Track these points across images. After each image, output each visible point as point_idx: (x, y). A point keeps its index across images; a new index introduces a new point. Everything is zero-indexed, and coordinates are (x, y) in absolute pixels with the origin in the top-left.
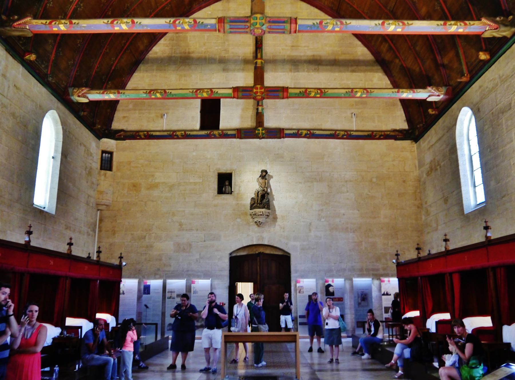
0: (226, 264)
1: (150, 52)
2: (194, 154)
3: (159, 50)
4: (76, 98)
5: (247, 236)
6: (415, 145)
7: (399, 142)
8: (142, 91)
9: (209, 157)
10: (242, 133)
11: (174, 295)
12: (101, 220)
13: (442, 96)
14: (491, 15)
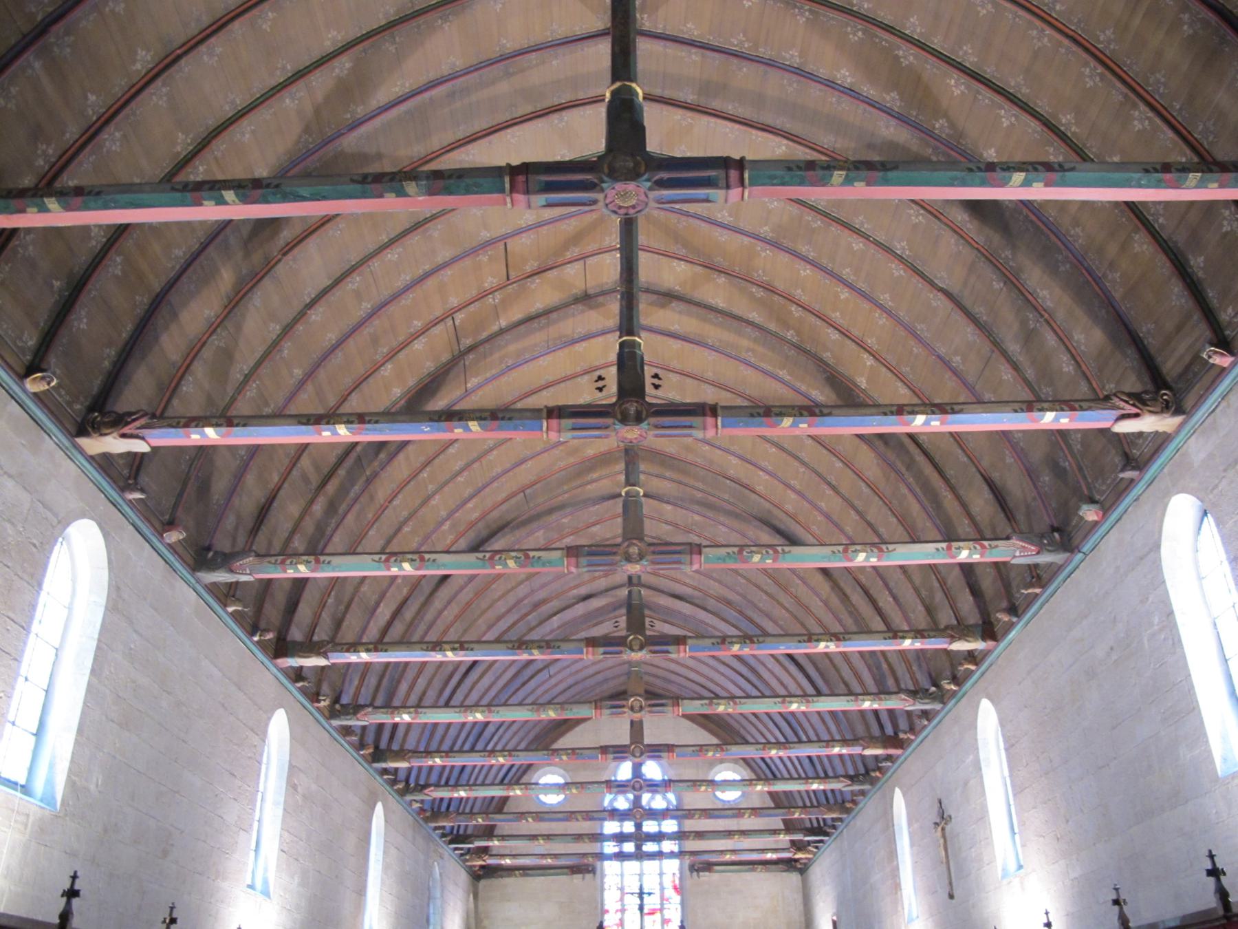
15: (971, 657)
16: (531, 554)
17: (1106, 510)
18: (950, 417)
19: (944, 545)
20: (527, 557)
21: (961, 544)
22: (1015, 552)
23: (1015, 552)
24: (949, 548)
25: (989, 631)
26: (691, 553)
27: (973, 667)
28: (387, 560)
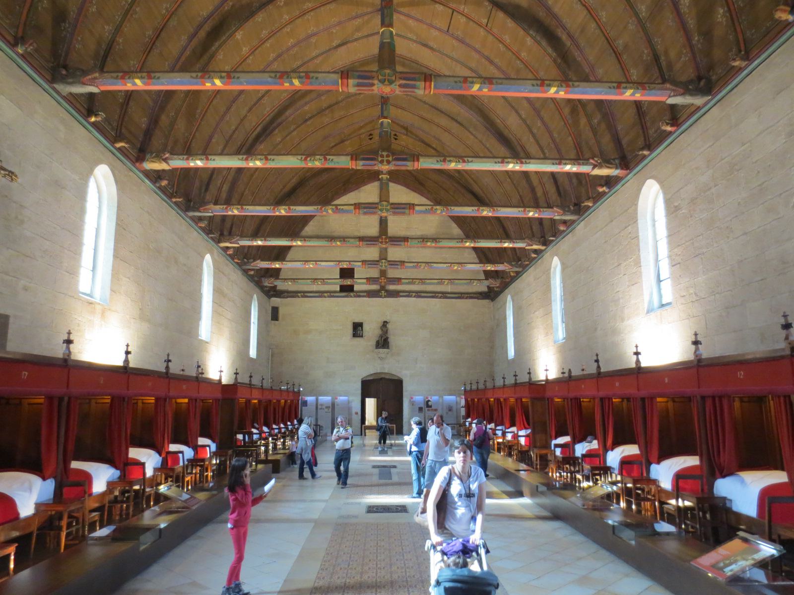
0: (359, 386)
1: (303, 231)
2: (336, 308)
3: (309, 229)
4: (266, 284)
5: (372, 365)
6: (492, 303)
7: (480, 301)
8: (309, 280)
9: (347, 311)
10: (371, 294)
11: (324, 407)
12: (272, 356)
13: (498, 285)
14: (509, 263)
15: (535, 251)
16: (339, 207)
17: (595, 203)
18: (524, 165)
19: (522, 209)
20: (337, 208)
21: (530, 209)
22: (555, 214)
23: (555, 214)
24: (524, 211)
25: (546, 243)
26: (410, 209)
27: (535, 256)
28: (274, 209)
